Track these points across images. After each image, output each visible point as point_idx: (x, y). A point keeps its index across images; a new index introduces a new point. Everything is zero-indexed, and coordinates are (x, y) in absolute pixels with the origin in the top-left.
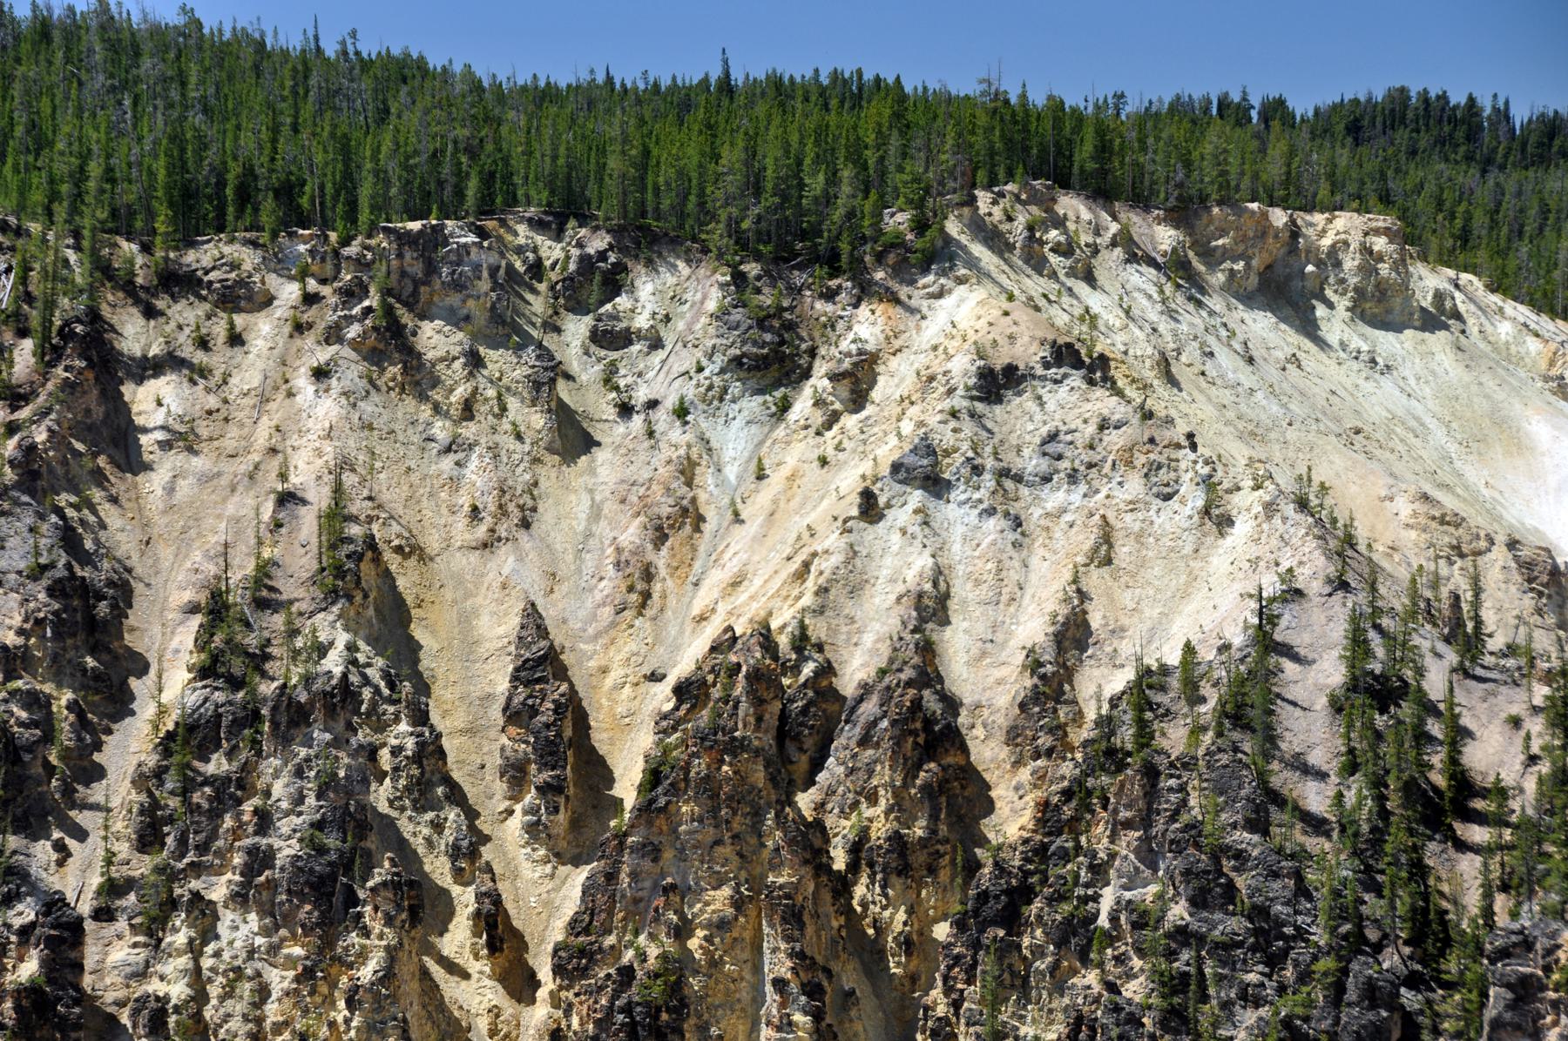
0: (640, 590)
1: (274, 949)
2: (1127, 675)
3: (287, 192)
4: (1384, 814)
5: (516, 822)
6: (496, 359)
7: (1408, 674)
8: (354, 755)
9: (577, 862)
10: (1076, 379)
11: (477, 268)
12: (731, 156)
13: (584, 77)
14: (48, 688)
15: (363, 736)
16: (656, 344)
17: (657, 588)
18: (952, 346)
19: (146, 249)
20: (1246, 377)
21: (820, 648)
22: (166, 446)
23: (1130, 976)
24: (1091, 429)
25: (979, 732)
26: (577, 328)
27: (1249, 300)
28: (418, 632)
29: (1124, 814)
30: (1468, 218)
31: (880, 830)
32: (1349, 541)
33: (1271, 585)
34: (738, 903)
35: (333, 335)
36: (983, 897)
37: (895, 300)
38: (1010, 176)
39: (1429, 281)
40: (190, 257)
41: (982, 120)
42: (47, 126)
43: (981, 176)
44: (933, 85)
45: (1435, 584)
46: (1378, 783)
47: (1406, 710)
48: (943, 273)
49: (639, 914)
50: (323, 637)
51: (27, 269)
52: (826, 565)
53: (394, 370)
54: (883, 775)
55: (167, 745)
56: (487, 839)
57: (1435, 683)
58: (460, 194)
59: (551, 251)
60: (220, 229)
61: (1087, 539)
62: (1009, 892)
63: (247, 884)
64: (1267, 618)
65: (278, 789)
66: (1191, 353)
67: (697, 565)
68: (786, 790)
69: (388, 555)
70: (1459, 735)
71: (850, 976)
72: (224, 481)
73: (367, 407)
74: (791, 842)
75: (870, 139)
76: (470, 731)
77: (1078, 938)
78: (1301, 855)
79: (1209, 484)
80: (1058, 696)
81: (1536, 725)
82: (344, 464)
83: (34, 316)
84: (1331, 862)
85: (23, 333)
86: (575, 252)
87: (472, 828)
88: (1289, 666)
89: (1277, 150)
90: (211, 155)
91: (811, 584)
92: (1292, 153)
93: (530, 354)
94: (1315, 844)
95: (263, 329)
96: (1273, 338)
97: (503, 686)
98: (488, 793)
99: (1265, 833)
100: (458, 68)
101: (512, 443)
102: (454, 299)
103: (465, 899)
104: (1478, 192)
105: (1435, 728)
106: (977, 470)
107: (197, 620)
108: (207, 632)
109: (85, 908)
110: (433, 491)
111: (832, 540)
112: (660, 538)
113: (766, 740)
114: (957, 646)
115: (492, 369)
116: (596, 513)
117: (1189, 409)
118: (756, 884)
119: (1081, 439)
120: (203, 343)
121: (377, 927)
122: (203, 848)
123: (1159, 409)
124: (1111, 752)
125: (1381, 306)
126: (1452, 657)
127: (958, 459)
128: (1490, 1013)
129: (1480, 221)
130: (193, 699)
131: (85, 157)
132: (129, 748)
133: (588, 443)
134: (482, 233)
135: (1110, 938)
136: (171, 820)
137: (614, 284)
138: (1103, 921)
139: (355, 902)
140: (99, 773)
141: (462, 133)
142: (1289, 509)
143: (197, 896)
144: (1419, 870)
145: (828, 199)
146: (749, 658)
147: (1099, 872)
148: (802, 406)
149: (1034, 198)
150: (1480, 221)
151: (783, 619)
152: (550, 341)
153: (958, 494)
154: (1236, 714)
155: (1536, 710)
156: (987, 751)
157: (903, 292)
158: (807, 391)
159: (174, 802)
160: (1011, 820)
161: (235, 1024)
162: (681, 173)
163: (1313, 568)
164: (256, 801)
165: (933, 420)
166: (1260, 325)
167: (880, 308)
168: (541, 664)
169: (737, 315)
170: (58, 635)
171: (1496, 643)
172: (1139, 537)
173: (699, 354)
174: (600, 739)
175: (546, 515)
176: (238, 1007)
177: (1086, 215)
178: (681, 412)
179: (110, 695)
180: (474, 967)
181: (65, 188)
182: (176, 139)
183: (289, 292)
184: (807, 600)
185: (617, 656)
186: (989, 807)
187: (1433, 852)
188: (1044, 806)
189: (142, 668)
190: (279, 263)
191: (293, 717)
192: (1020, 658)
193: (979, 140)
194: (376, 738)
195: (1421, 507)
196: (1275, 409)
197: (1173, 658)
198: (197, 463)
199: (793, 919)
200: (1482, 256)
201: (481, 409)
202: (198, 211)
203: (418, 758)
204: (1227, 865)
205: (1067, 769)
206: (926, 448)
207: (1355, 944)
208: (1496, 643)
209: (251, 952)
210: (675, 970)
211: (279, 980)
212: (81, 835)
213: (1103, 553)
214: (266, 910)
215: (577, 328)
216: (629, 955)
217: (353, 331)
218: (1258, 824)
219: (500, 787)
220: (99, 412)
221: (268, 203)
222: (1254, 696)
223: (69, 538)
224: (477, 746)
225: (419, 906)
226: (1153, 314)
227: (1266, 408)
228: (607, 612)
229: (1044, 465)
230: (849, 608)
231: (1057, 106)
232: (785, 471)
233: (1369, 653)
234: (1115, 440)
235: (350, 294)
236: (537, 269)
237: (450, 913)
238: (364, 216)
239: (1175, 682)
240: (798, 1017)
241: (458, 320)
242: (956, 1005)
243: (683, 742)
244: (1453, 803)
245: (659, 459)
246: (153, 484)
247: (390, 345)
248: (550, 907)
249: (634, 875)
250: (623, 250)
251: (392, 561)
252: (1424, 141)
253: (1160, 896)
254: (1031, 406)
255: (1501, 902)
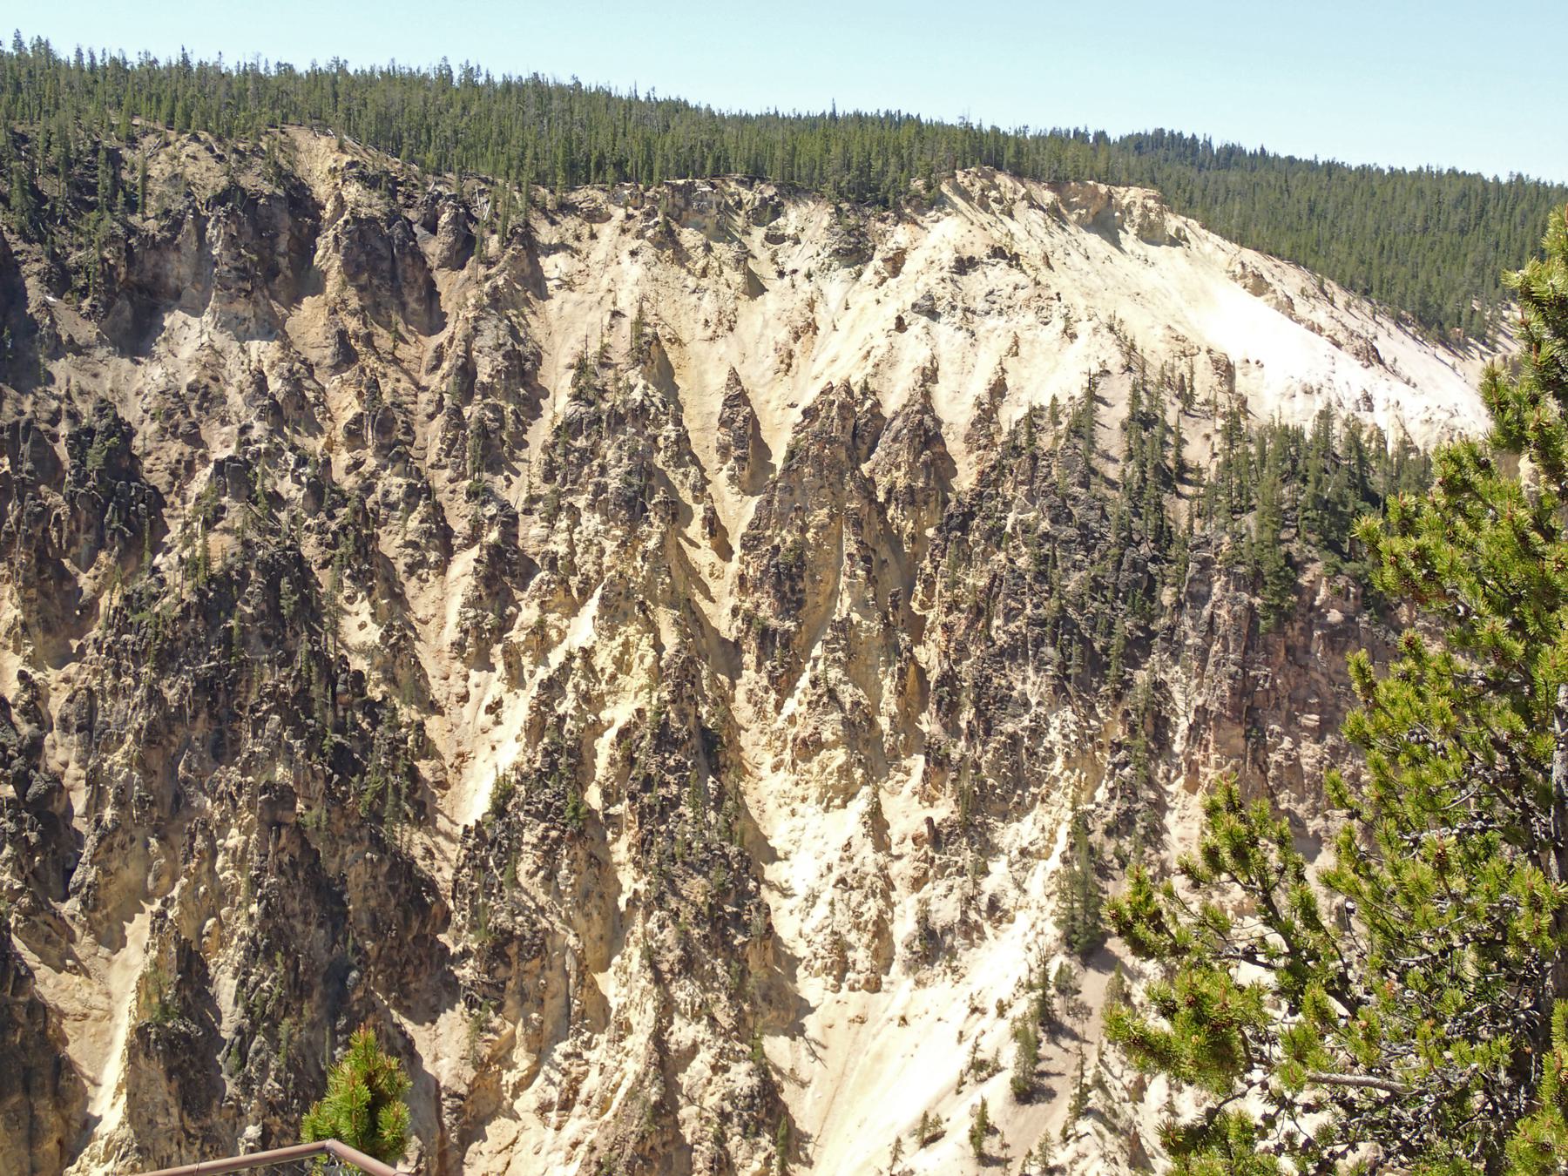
0: (787, 362)
1: (607, 531)
2: (1026, 410)
3: (619, 165)
4: (1145, 480)
5: (725, 474)
6: (718, 247)
7: (1159, 413)
8: (646, 440)
9: (753, 494)
10: (1003, 264)
11: (710, 203)
12: (836, 150)
13: (765, 111)
14: (502, 403)
15: (650, 431)
16: (797, 242)
17: (794, 362)
18: (943, 246)
19: (552, 192)
20: (1085, 265)
21: (874, 393)
22: (559, 287)
23: (1020, 555)
24: (1010, 289)
25: (951, 436)
26: (759, 233)
27: (1088, 228)
28: (678, 381)
29: (1020, 478)
30: (1192, 193)
31: (901, 484)
32: (1133, 347)
33: (1096, 369)
34: (831, 517)
35: (640, 235)
36: (951, 516)
37: (916, 223)
38: (973, 164)
39: (1173, 222)
40: (573, 196)
41: (960, 137)
42: (508, 134)
43: (959, 163)
44: (936, 119)
45: (1172, 370)
46: (1143, 465)
47: (1157, 430)
48: (939, 210)
49: (783, 520)
50: (632, 382)
51: (496, 201)
52: (877, 354)
53: (669, 252)
54: (904, 456)
55: (557, 432)
56: (709, 482)
57: (1171, 417)
58: (703, 167)
59: (747, 195)
60: (588, 182)
61: (1009, 343)
62: (963, 514)
63: (595, 500)
64: (1093, 384)
65: (610, 455)
66: (1059, 253)
67: (815, 352)
68: (856, 463)
69: (664, 343)
70: (1182, 442)
71: (885, 553)
72: (586, 305)
73: (655, 270)
74: (858, 488)
75: (905, 144)
76: (702, 429)
77: (996, 536)
78: (1104, 499)
79: (1067, 318)
80: (990, 420)
81: (1217, 439)
82: (644, 298)
83: (499, 224)
84: (1118, 502)
85: (493, 232)
86: (758, 196)
87: (703, 477)
88: (1101, 406)
89: (1102, 156)
90: (584, 148)
91: (871, 361)
92: (1109, 158)
93: (735, 246)
94: (1111, 493)
95: (607, 231)
96: (1099, 248)
97: (718, 408)
98: (711, 459)
99: (1088, 488)
100: (703, 106)
101: (724, 289)
102: (699, 218)
103: (699, 511)
104: (1197, 181)
105: (1170, 439)
106: (954, 308)
107: (573, 372)
108: (577, 378)
109: (519, 508)
110: (687, 312)
111: (881, 343)
112: (797, 338)
113: (848, 438)
114: (941, 394)
115: (716, 253)
116: (766, 324)
117: (1056, 281)
118: (840, 508)
119: (1005, 294)
120: (578, 238)
121: (656, 522)
122: (574, 482)
123: (1044, 282)
124: (1015, 448)
125: (1151, 234)
126: (1179, 405)
127: (944, 302)
128: (1189, 575)
129: (1197, 195)
130: (570, 411)
131: (525, 148)
132: (540, 433)
133: (763, 290)
134: (713, 186)
135: (1011, 538)
136: (559, 468)
137: (777, 212)
138: (1008, 529)
139: (646, 510)
140: (526, 444)
141: (705, 137)
142: (1105, 331)
143: (571, 505)
144: (1160, 507)
145: (883, 173)
146: (838, 397)
147: (1007, 505)
148: (868, 274)
149: (985, 175)
150: (1197, 195)
151: (857, 381)
152: (745, 239)
153: (942, 320)
154: (1076, 431)
155: (1217, 431)
156: (955, 446)
157: (919, 219)
158: (871, 264)
159: (560, 460)
160: (965, 480)
161: (589, 566)
162: (812, 160)
163: (1115, 360)
164: (599, 460)
165: (933, 283)
166: (1093, 241)
167: (909, 227)
168: (737, 398)
169: (837, 228)
170: (507, 377)
171: (1200, 399)
172: (1032, 342)
173: (818, 247)
174: (765, 435)
175: (741, 327)
176: (590, 558)
177: (1010, 184)
178: (809, 276)
179: (531, 407)
180: (702, 543)
181: (515, 163)
182: (568, 139)
183: (619, 214)
184: (870, 370)
185: (774, 395)
186: (955, 473)
187: (1167, 498)
188: (982, 473)
189: (547, 395)
190: (615, 199)
191: (617, 420)
192: (972, 401)
193: (958, 146)
194: (657, 432)
195: (1168, 332)
196: (1098, 281)
197: (1047, 403)
198: (574, 296)
199: (858, 524)
200: (1198, 212)
201: (711, 272)
202: (577, 173)
203: (677, 442)
204: (1069, 503)
205: (993, 455)
206: (929, 297)
207: (1129, 542)
208: (1200, 399)
209: (597, 532)
210: (800, 548)
211: (610, 546)
212: (517, 474)
213: (1014, 351)
214: (604, 513)
215: (759, 233)
216: (777, 540)
217: (650, 233)
218: (1085, 484)
219: (716, 457)
220: (528, 270)
221: (611, 170)
222: (1085, 421)
223: (513, 331)
224: (706, 437)
225: (676, 513)
226: (1041, 233)
227: (1094, 281)
228: (770, 374)
229: (986, 306)
230: (889, 374)
231: (995, 130)
232: (860, 305)
233: (1140, 402)
234: (1021, 295)
235: (649, 215)
236: (739, 204)
237: (691, 516)
238: (656, 177)
239: (1047, 414)
240: (859, 572)
241: (700, 228)
242: (936, 568)
243: (806, 438)
244: (1176, 475)
245: (797, 298)
246: (552, 306)
247: (667, 240)
248: (739, 516)
249: (780, 502)
250: (782, 195)
251: (666, 345)
252: (1171, 155)
253: (1036, 518)
254: (981, 277)
255: (1197, 522)
